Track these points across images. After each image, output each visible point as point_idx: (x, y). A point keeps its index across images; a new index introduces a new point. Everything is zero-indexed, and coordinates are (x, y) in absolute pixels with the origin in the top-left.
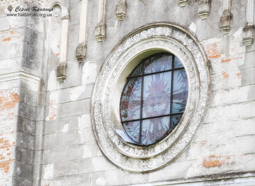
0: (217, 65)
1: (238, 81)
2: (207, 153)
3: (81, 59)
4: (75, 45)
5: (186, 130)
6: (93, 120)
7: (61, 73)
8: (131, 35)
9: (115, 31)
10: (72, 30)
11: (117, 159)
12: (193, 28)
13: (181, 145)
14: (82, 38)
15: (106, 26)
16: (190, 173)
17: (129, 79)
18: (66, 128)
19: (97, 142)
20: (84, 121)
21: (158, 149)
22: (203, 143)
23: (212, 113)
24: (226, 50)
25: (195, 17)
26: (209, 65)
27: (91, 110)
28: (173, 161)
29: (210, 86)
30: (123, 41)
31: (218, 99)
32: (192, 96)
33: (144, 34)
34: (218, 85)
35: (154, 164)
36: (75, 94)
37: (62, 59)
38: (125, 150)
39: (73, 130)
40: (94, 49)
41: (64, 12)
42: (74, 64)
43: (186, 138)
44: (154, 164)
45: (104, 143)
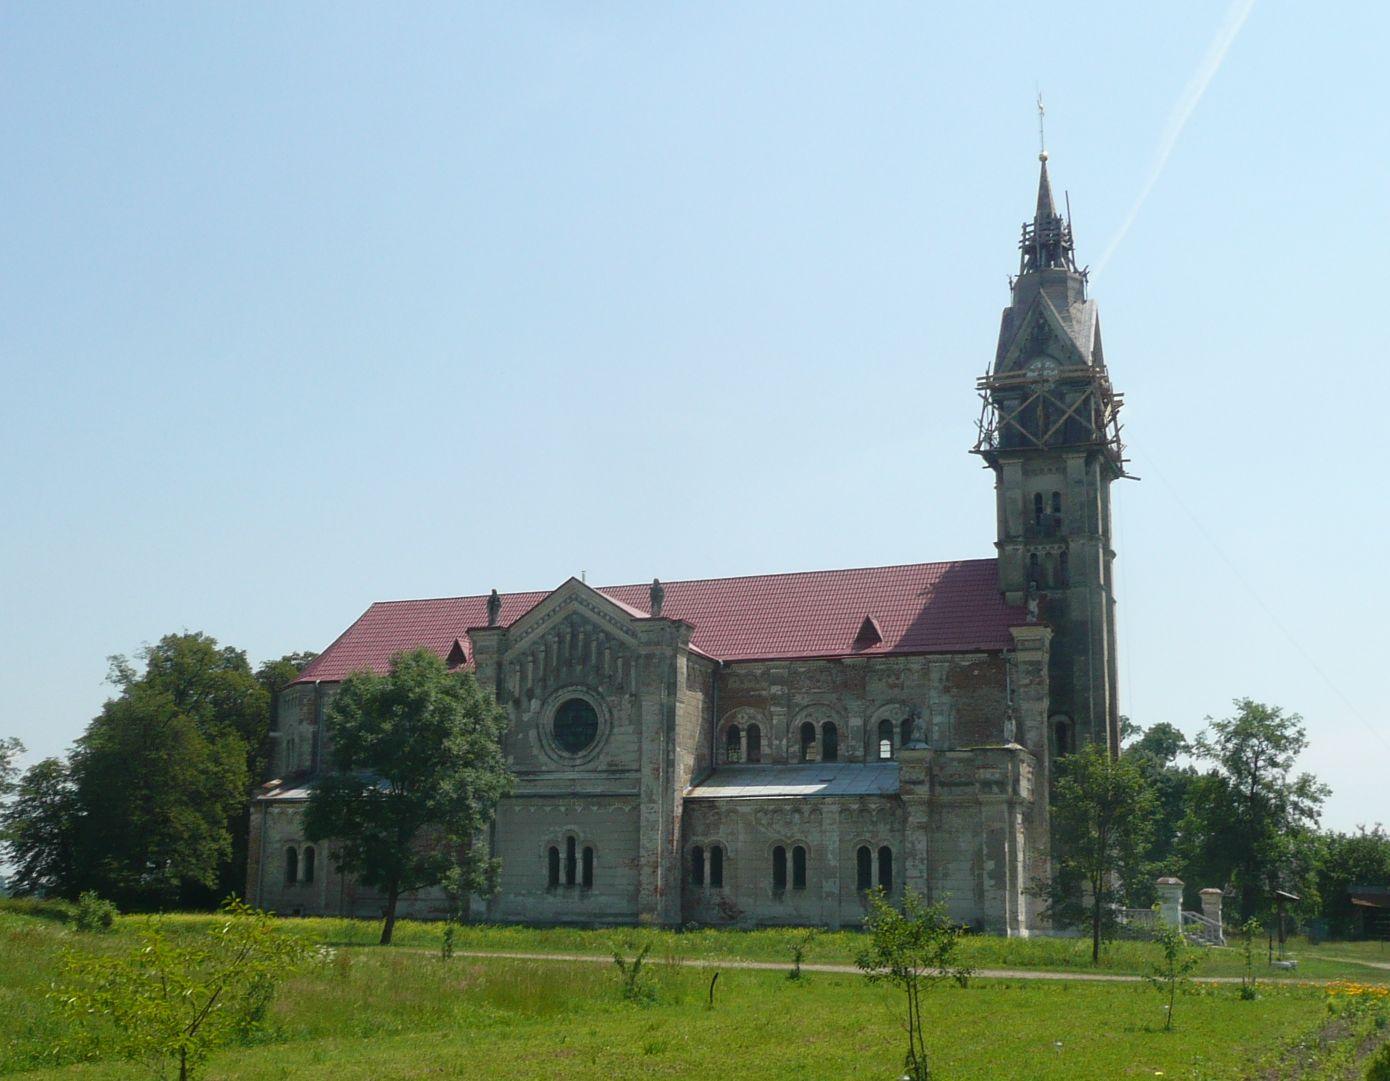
0: (615, 712)
1: (627, 723)
2: (609, 759)
4: (525, 690)
5: (597, 745)
6: (538, 733)
8: (562, 687)
9: (551, 682)
10: (523, 678)
11: (555, 757)
12: (600, 689)
13: (594, 754)
14: (529, 685)
15: (545, 680)
16: (600, 769)
18: (520, 736)
19: (542, 746)
20: (532, 733)
21: (581, 754)
22: (607, 754)
23: (612, 738)
24: (620, 704)
25: (601, 684)
26: (610, 712)
27: (538, 728)
28: (590, 761)
29: (611, 723)
30: (556, 690)
31: (616, 730)
32: (601, 727)
33: (570, 688)
34: (616, 723)
35: (578, 762)
36: (526, 717)
37: (517, 695)
38: (559, 753)
39: (526, 736)
40: (538, 691)
41: (518, 668)
42: (524, 700)
43: (597, 750)
44: (578, 762)
45: (547, 748)
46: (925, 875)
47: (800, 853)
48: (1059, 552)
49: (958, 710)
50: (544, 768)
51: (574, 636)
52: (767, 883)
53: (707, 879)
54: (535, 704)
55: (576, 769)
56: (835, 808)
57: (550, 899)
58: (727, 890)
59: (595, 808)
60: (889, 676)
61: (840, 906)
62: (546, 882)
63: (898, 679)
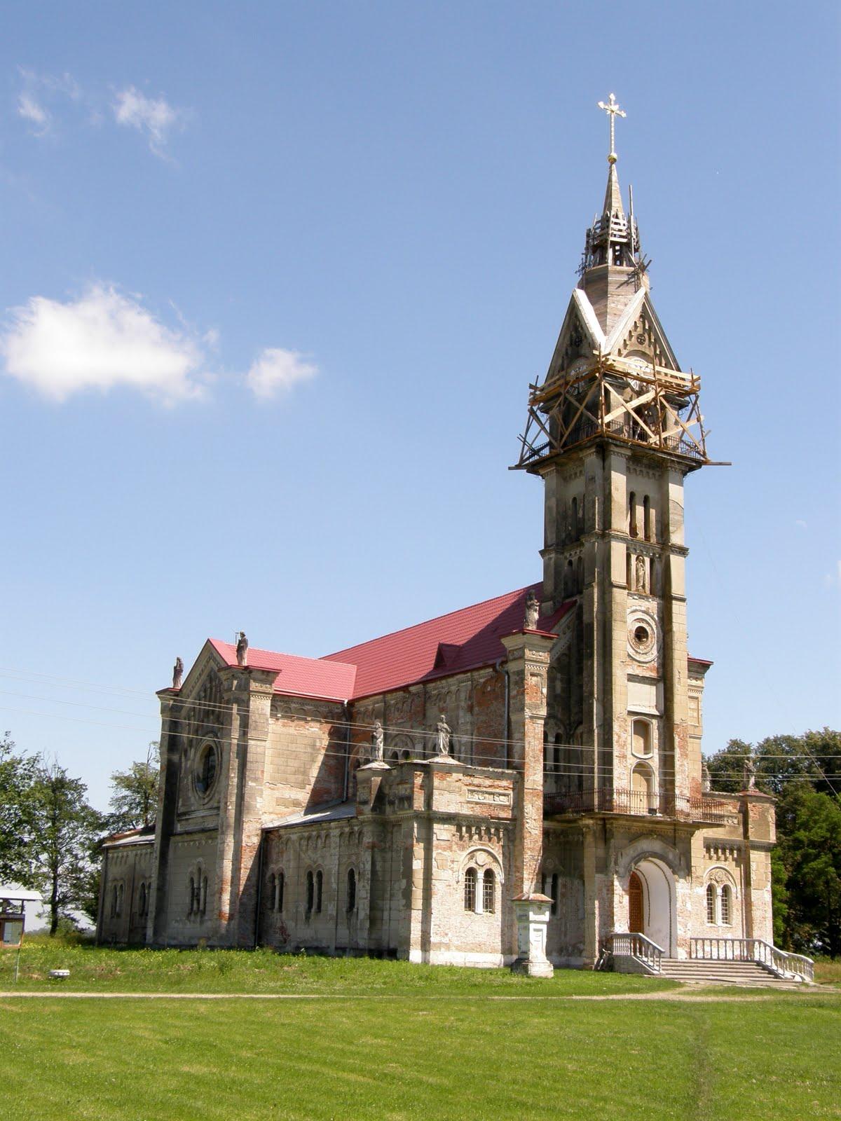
3: (191, 746)
7: (186, 751)
17: (206, 757)
20: (190, 777)
35: (206, 801)
42: (189, 749)
44: (206, 801)
46: (369, 895)
47: (320, 875)
48: (577, 557)
49: (478, 728)
50: (193, 808)
51: (211, 689)
52: (303, 907)
53: (277, 905)
54: (193, 750)
55: (206, 807)
56: (336, 832)
57: (189, 925)
58: (284, 913)
59: (210, 841)
60: (440, 701)
61: (336, 929)
62: (187, 910)
63: (445, 702)
